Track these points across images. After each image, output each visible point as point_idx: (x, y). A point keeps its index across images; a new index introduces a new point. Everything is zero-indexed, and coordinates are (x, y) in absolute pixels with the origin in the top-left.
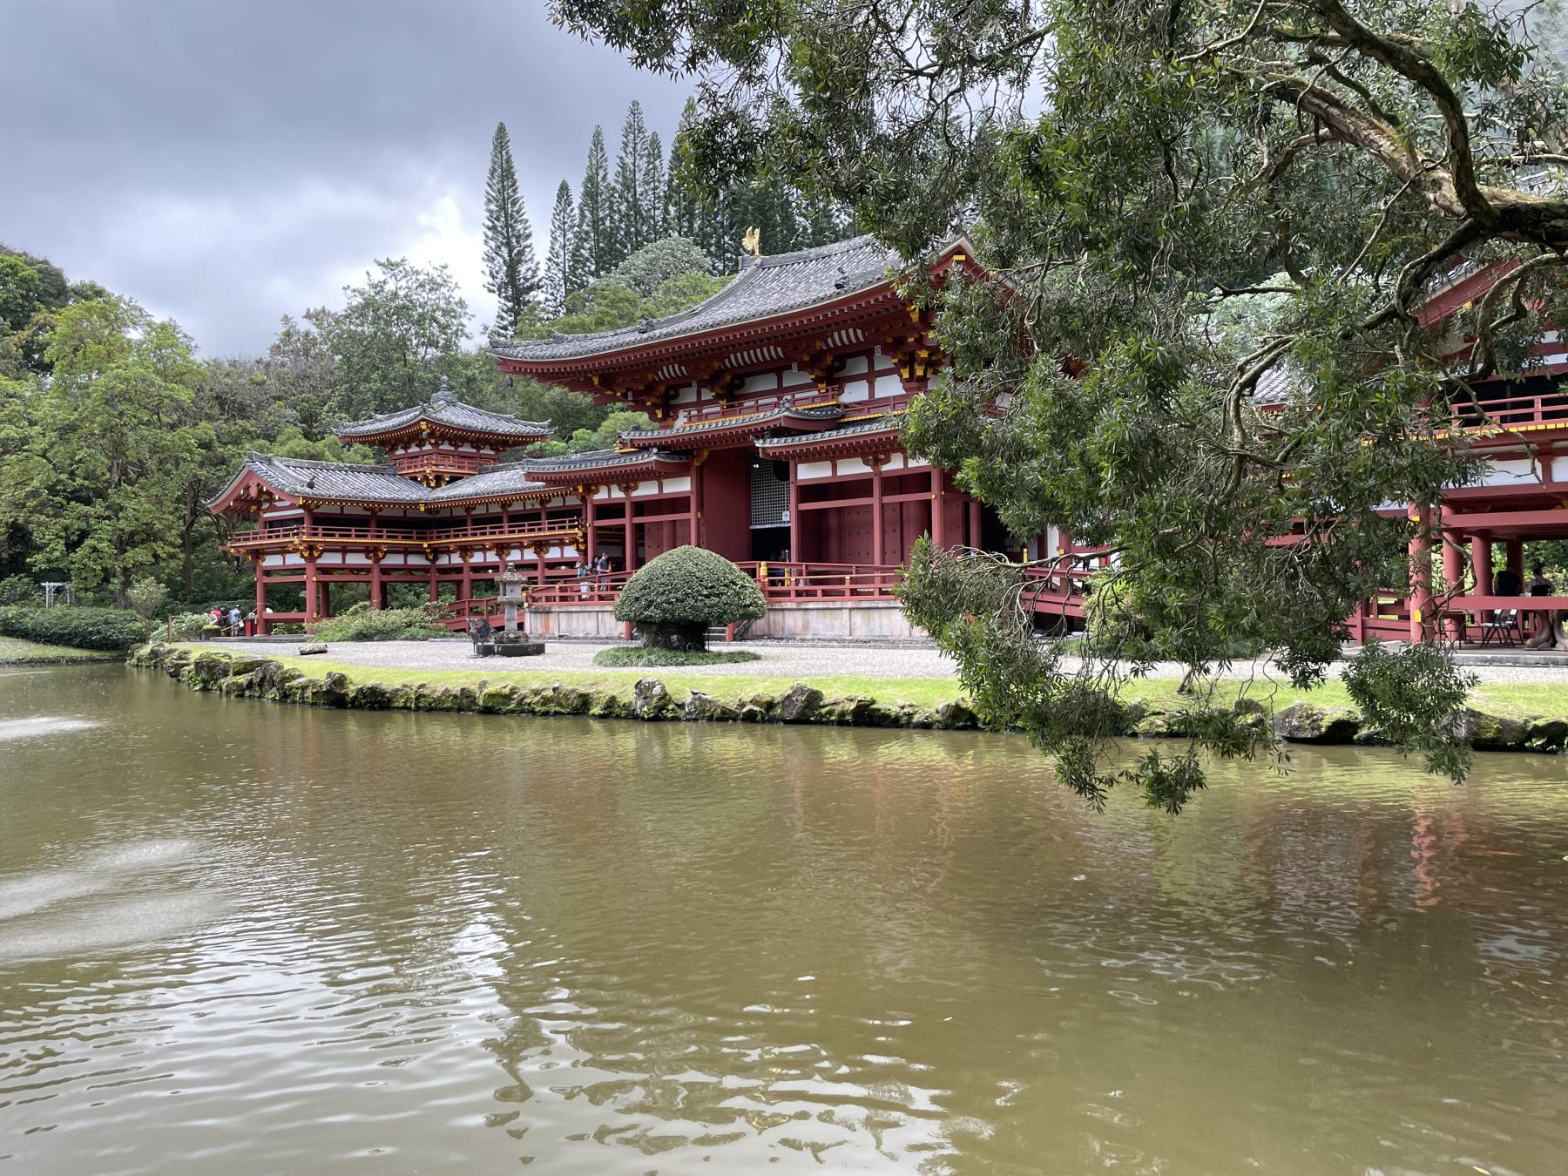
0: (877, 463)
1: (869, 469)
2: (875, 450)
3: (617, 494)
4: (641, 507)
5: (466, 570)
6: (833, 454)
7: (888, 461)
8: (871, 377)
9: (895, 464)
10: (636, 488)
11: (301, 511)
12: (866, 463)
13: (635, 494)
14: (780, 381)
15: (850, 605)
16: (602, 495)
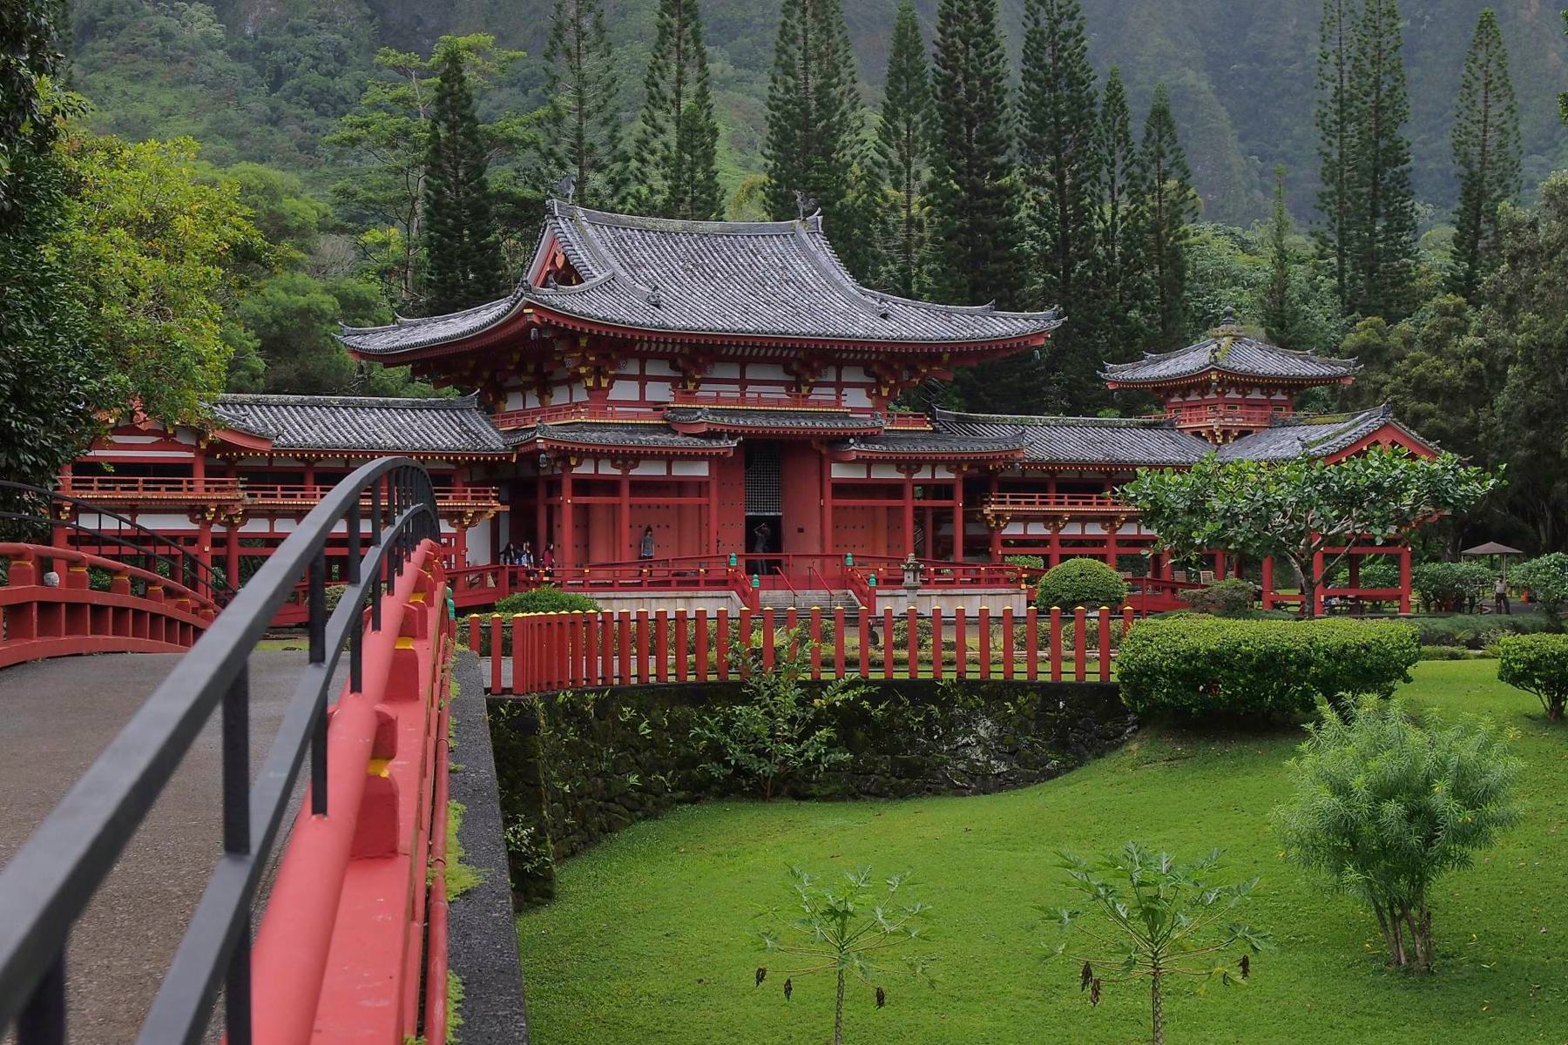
0: (910, 472)
1: (902, 476)
2: (910, 464)
3: (607, 470)
4: (643, 487)
5: (234, 542)
6: (869, 463)
7: (918, 470)
8: (839, 386)
9: (924, 475)
10: (635, 466)
11: (191, 455)
12: (899, 470)
13: (632, 472)
14: (743, 373)
15: (939, 592)
16: (586, 469)
